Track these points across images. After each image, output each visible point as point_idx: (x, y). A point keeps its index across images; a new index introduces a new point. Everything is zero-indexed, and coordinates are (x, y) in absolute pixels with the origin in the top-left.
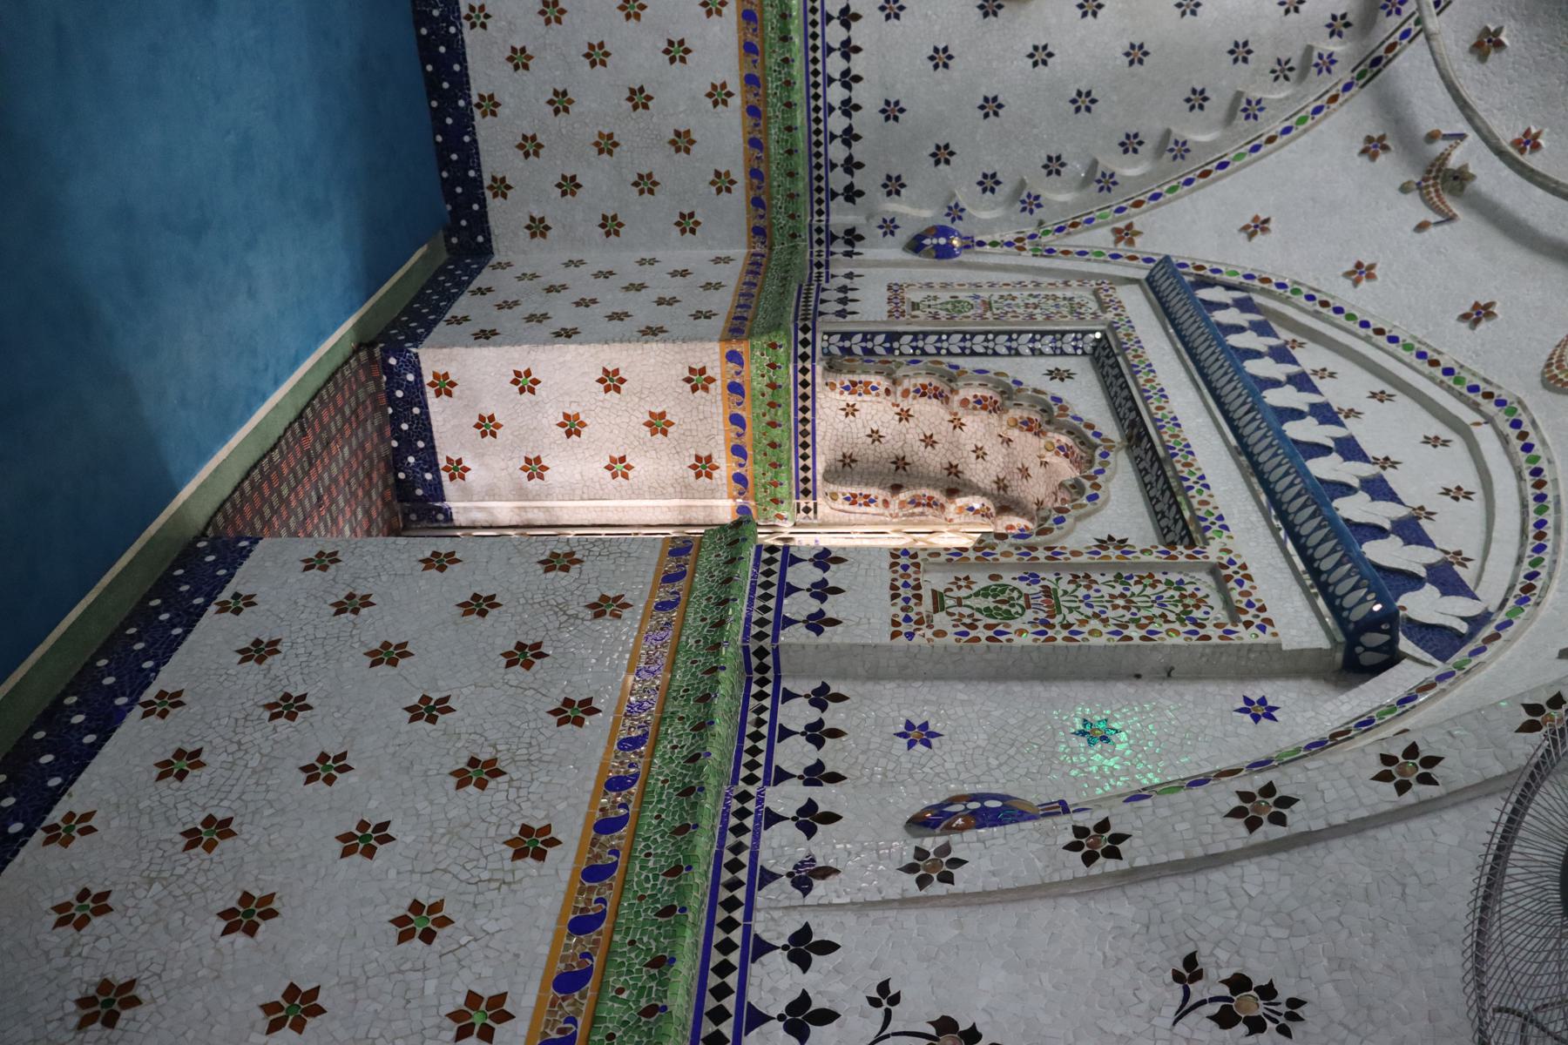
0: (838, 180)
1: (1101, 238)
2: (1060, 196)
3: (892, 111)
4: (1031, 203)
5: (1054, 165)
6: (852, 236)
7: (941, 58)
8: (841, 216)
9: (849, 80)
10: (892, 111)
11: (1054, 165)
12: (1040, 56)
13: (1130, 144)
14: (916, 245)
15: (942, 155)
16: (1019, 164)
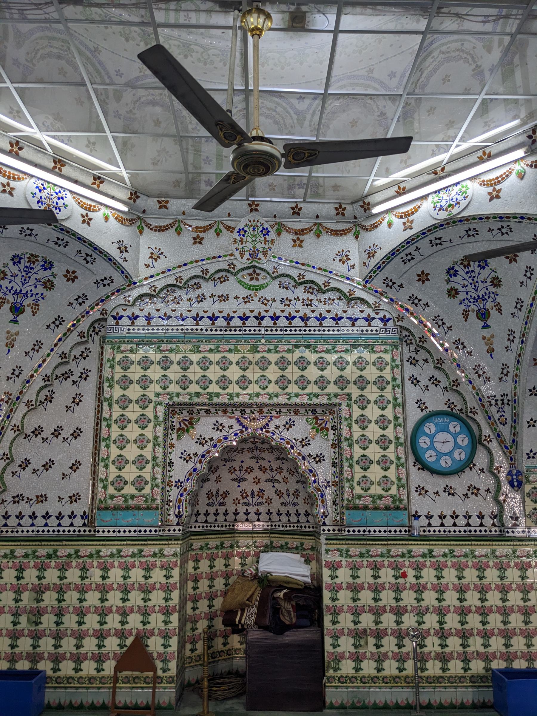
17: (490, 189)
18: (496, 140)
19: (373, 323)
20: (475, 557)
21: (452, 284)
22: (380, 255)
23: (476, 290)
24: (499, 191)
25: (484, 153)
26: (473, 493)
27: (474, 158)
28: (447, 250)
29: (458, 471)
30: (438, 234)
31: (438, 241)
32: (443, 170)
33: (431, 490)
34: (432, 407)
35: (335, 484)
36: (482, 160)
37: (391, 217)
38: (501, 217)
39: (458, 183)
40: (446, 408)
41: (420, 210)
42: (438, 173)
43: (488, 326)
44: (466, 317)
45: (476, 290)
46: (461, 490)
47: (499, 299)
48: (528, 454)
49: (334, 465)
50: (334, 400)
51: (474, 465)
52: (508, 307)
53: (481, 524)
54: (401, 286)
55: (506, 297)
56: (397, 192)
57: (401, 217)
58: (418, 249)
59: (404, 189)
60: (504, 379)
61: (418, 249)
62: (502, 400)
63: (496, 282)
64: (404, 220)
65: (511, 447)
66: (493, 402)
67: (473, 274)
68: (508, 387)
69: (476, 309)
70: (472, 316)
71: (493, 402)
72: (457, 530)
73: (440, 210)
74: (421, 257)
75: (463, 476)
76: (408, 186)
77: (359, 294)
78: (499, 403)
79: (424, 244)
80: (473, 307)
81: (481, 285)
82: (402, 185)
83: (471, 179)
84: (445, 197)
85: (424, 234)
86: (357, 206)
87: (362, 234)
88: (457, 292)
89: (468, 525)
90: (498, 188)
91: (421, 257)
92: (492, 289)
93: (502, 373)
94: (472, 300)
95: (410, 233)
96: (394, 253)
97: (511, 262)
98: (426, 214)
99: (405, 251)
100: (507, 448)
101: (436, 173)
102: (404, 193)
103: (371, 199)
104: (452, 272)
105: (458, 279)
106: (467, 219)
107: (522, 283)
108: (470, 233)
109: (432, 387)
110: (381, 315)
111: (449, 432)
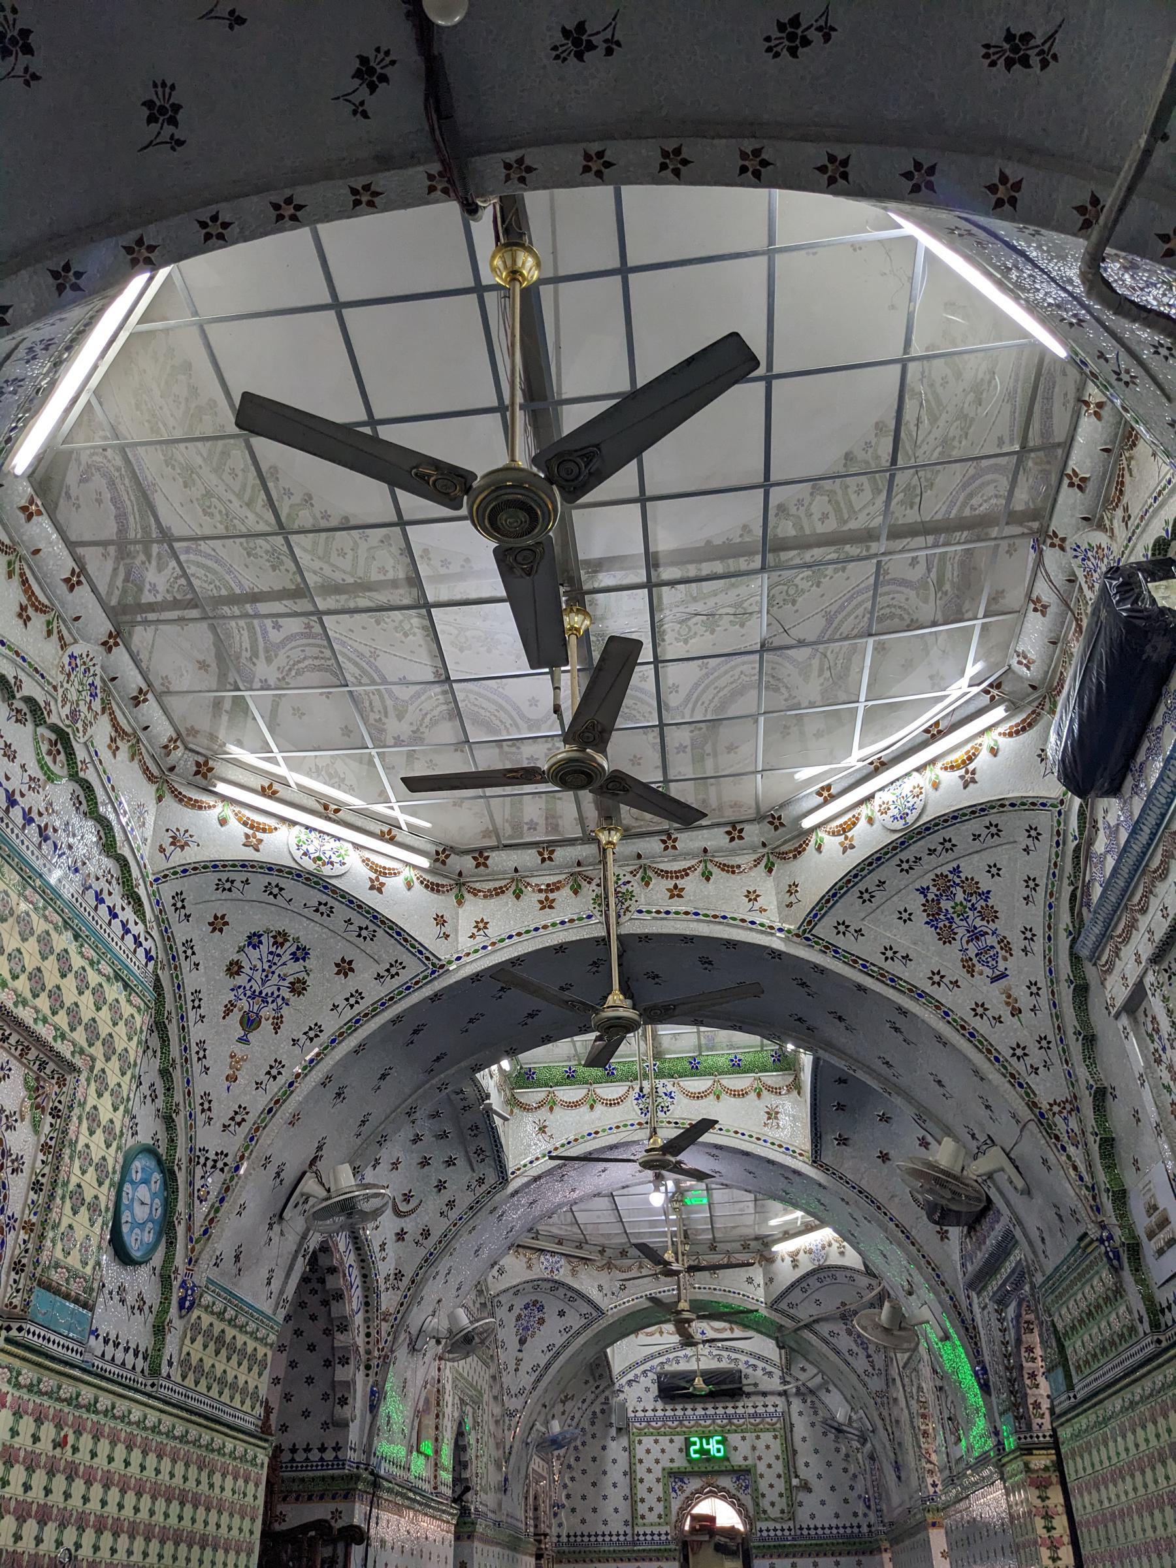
0: (856, 1530)
1: (859, 1456)
2: (852, 1469)
3: (837, 1516)
4: (855, 1476)
5: (845, 1470)
6: (869, 1526)
7: (823, 1503)
8: (865, 1529)
9: (830, 1528)
10: (837, 1516)
11: (845, 1470)
12: (819, 1477)
13: (838, 1450)
14: (869, 1507)
15: (846, 1501)
16: (846, 1480)
17: (374, 876)
18: (414, 830)
21: (242, 957)
22: (191, 855)
23: (264, 982)
24: (383, 884)
25: (390, 832)
27: (376, 828)
28: (273, 908)
30: (283, 883)
31: (276, 891)
32: (337, 811)
35: (29, 1227)
36: (381, 837)
37: (228, 811)
38: (375, 917)
39: (339, 839)
41: (275, 833)
42: (328, 810)
43: (247, 1042)
44: (227, 1012)
45: (264, 982)
47: (285, 1011)
49: (36, 1187)
50: (78, 1061)
52: (293, 1026)
54: (187, 917)
55: (298, 1015)
56: (263, 788)
57: (245, 824)
58: (247, 882)
59: (275, 792)
60: (232, 1128)
61: (247, 882)
62: (215, 1161)
63: (298, 987)
64: (250, 832)
65: (198, 1241)
66: (202, 1160)
67: (276, 959)
68: (233, 1143)
69: (246, 1009)
70: (236, 1016)
71: (202, 1160)
73: (305, 854)
74: (240, 896)
76: (283, 792)
77: (141, 891)
78: (210, 1163)
79: (259, 881)
80: (244, 1004)
81: (275, 979)
82: (276, 787)
83: (357, 846)
84: (316, 843)
85: (270, 869)
86: (192, 759)
87: (168, 799)
88: (238, 973)
90: (382, 879)
91: (240, 896)
92: (285, 993)
93: (232, 1119)
94: (249, 993)
95: (249, 854)
96: (215, 866)
97: (338, 973)
98: (283, 844)
99: (229, 874)
100: (191, 1240)
101: (326, 807)
102: (270, 797)
103: (219, 768)
104: (255, 940)
105: (254, 954)
106: (335, 890)
107: (335, 1007)
108: (322, 908)
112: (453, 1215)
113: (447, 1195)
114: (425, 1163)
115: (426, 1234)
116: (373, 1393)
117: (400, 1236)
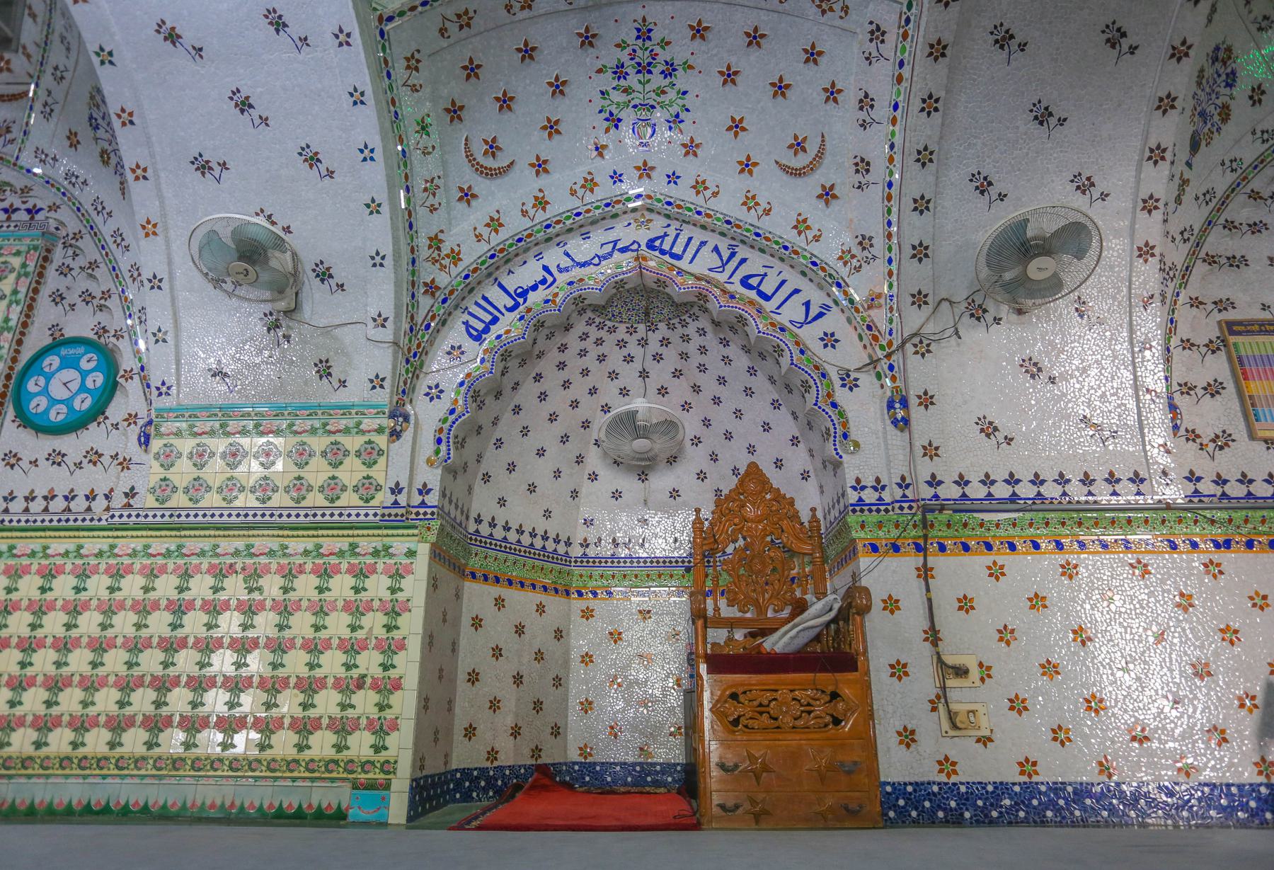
19: (14, 217)
20: (46, 556)
26: (90, 461)
29: (76, 424)
33: (26, 456)
34: (69, 333)
40: (91, 335)
46: (74, 455)
48: (158, 389)
51: (106, 418)
53: (89, 509)
72: (47, 518)
75: (84, 434)
89: (68, 510)
109: (80, 305)
110: (29, 205)
111: (78, 368)
112: (882, 111)
113: (850, 98)
114: (781, 88)
115: (863, 165)
116: (890, 406)
117: (828, 195)
